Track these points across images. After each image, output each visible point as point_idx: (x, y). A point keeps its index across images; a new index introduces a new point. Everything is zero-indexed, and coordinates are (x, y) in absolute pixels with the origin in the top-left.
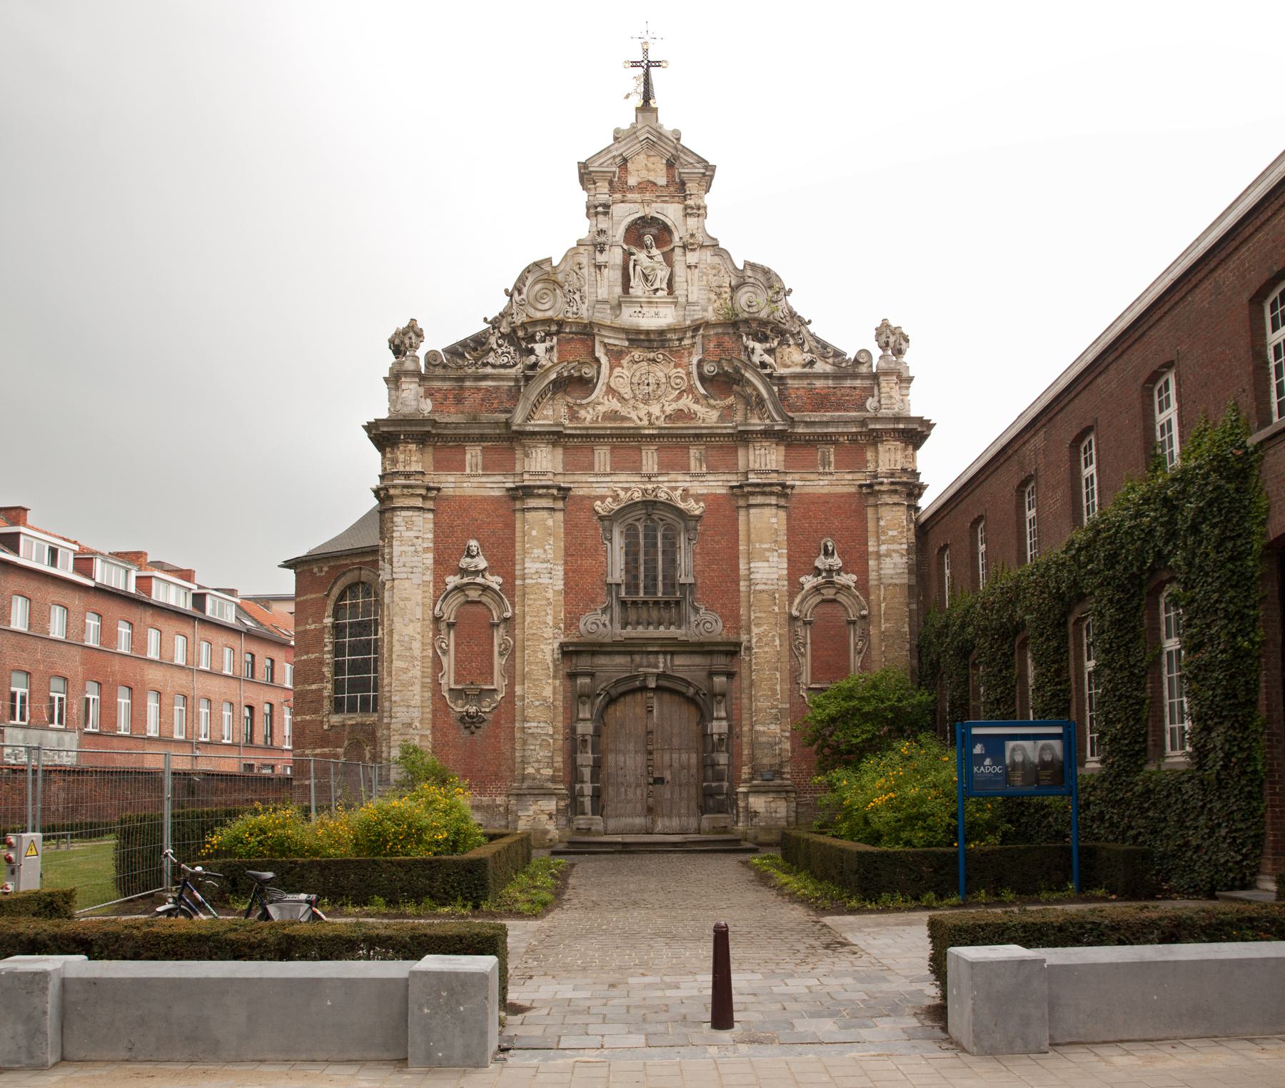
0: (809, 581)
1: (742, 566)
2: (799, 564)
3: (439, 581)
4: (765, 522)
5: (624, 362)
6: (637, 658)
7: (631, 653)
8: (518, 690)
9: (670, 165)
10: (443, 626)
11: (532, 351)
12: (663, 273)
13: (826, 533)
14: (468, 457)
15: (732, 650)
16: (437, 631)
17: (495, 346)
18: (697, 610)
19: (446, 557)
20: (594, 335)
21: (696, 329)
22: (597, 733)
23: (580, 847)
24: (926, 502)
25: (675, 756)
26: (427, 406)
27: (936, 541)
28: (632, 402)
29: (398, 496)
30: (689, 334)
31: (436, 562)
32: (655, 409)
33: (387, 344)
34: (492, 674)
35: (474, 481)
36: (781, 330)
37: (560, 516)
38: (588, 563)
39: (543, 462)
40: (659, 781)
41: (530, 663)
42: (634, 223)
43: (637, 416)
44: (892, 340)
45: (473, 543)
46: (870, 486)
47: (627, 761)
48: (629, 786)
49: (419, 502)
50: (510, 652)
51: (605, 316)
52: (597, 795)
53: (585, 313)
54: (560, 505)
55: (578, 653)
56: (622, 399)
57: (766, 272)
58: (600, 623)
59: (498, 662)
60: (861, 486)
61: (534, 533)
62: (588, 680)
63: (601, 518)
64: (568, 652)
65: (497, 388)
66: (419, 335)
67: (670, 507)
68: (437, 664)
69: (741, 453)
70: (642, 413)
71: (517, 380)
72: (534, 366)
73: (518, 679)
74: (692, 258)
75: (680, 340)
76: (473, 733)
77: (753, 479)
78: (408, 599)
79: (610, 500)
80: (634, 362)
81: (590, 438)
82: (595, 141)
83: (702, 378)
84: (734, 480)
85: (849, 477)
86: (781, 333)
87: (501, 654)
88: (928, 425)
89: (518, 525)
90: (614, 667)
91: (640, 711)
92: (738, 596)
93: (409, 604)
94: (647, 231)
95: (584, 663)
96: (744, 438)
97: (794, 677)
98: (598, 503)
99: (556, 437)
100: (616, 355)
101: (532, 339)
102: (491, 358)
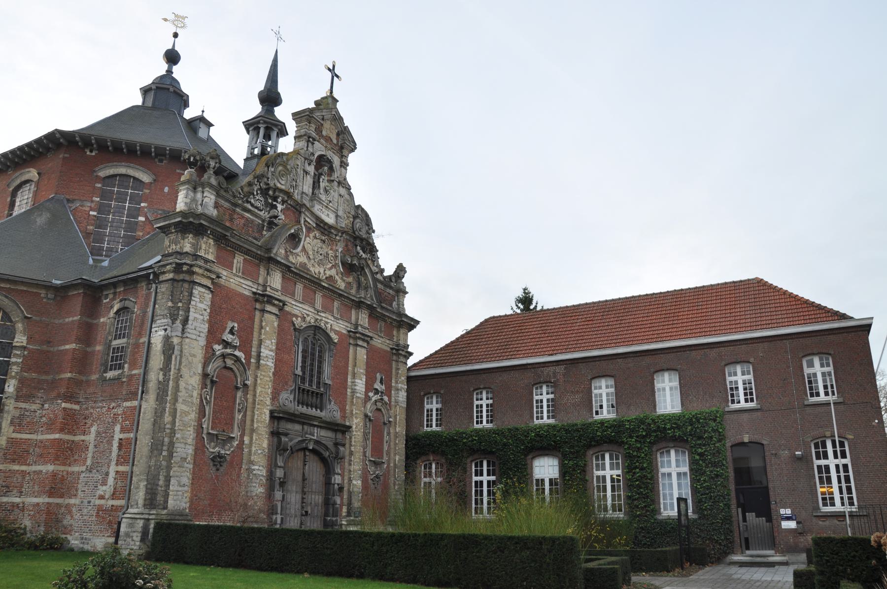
1: (349, 380)
3: (209, 348)
5: (311, 235)
6: (306, 427)
7: (303, 424)
10: (208, 382)
11: (275, 207)
14: (235, 261)
15: (344, 429)
16: (204, 386)
18: (330, 401)
20: (300, 212)
29: (198, 274)
31: (209, 331)
34: (232, 425)
38: (286, 357)
41: (258, 422)
43: (316, 270)
49: (208, 283)
55: (279, 419)
57: (367, 215)
59: (238, 417)
60: (392, 349)
61: (268, 329)
63: (295, 329)
65: (253, 221)
70: (317, 271)
71: (263, 221)
73: (247, 432)
76: (218, 470)
78: (194, 356)
79: (299, 319)
80: (315, 237)
87: (239, 411)
91: (300, 464)
93: (195, 360)
96: (359, 305)
98: (294, 319)
100: (309, 230)
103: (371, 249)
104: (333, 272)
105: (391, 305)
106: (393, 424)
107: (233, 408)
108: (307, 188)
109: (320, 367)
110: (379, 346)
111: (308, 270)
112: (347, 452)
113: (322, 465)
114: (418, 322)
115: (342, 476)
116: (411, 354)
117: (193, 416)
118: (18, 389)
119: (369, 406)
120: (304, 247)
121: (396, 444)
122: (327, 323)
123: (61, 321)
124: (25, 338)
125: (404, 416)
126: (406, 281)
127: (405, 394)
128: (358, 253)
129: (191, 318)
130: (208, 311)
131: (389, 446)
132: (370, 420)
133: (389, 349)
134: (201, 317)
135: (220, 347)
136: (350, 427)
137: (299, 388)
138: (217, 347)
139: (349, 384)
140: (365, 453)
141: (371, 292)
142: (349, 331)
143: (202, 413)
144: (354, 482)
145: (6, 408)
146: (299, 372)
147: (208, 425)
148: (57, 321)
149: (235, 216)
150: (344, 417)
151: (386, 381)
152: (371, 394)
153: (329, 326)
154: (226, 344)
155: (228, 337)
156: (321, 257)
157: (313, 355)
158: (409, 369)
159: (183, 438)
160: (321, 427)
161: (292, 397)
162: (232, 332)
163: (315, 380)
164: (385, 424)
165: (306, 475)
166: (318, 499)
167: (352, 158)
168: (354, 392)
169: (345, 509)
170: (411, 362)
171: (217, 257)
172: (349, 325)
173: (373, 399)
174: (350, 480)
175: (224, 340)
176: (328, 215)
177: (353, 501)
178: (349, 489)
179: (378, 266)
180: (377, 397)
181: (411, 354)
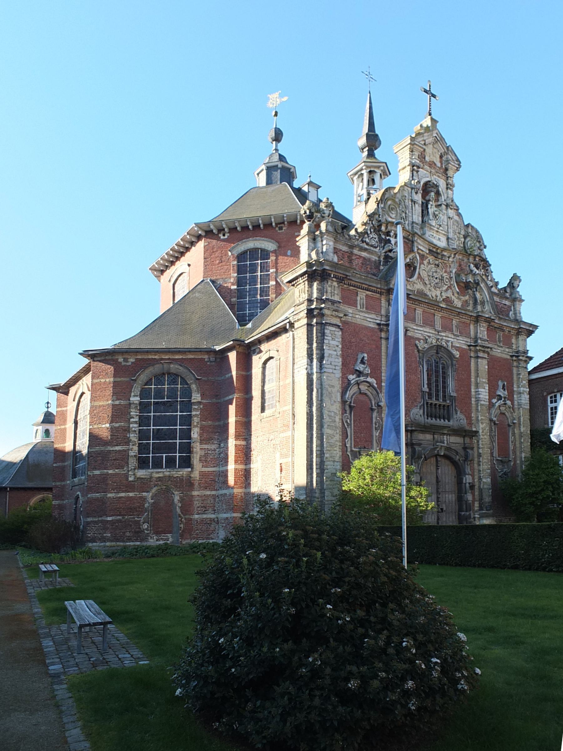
1: (473, 390)
3: (344, 377)
5: (425, 262)
10: (347, 408)
14: (359, 298)
16: (344, 411)
17: (369, 232)
20: (413, 242)
25: (447, 495)
28: (429, 286)
30: (453, 256)
46: (517, 357)
48: (429, 514)
49: (337, 321)
57: (477, 232)
59: (376, 434)
60: (512, 356)
63: (419, 351)
75: (449, 257)
78: (333, 386)
85: (507, 350)
87: (376, 429)
91: (433, 468)
92: (471, 407)
98: (417, 342)
103: (484, 264)
104: (449, 294)
105: (508, 315)
106: (517, 425)
107: (372, 427)
108: (417, 218)
109: (444, 382)
110: (499, 355)
111: (426, 295)
112: (476, 455)
113: (453, 468)
114: (536, 327)
115: (473, 476)
116: (531, 358)
117: (338, 437)
118: (201, 435)
119: (493, 411)
120: (419, 274)
121: (521, 443)
122: (448, 341)
123: (223, 378)
124: (199, 395)
125: (528, 417)
126: (522, 290)
127: (528, 397)
128: (472, 271)
129: (325, 355)
130: (340, 346)
131: (515, 445)
132: (495, 424)
133: (509, 357)
134: (335, 353)
135: (354, 376)
136: (477, 432)
137: (427, 403)
138: (351, 377)
139: (473, 393)
140: (492, 454)
141: (487, 307)
142: (469, 346)
143: (345, 435)
144: (484, 480)
145: (195, 450)
146: (426, 389)
147: (351, 444)
148: (219, 379)
149: (354, 258)
150: (470, 424)
151: (509, 388)
152: (494, 401)
153: (450, 344)
154: (359, 373)
155: (360, 367)
156: (437, 281)
157: (437, 372)
158: (530, 373)
159: (331, 457)
160: (450, 435)
161: (422, 411)
162: (362, 362)
163: (441, 394)
164: (509, 426)
165: (440, 479)
166: (451, 497)
167: (457, 178)
168: (478, 400)
169: (477, 504)
170: (531, 366)
171: (342, 298)
172: (469, 340)
173: (497, 404)
174: (480, 479)
175: (357, 370)
176: (439, 239)
177: (484, 496)
178: (479, 487)
179: (492, 280)
180: (501, 402)
181: (531, 358)
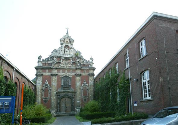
0: (83, 85)
2: (82, 83)
3: (43, 85)
4: (78, 78)
8: (51, 97)
9: (69, 40)
12: (68, 51)
13: (85, 79)
15: (75, 93)
16: (42, 91)
19: (43, 82)
21: (72, 57)
22: (60, 102)
23: (58, 116)
24: (95, 76)
26: (42, 65)
27: (96, 80)
32: (67, 66)
33: (38, 58)
35: (47, 74)
36: (80, 58)
37: (56, 78)
38: (59, 83)
39: (55, 72)
40: (67, 108)
42: (65, 46)
44: (92, 59)
45: (47, 81)
47: (63, 105)
50: (50, 93)
51: (62, 56)
52: (60, 110)
53: (60, 55)
54: (56, 76)
56: (63, 65)
57: (79, 52)
58: (60, 90)
62: (59, 96)
64: (57, 93)
66: (41, 57)
67: (68, 77)
68: (42, 95)
69: (76, 71)
72: (54, 61)
74: (71, 50)
77: (77, 74)
81: (60, 69)
82: (61, 36)
83: (72, 63)
84: (75, 74)
86: (80, 58)
88: (95, 68)
89: (52, 79)
90: (62, 95)
94: (67, 47)
95: (59, 94)
96: (76, 69)
97: (81, 95)
99: (56, 69)
101: (54, 58)
102: (49, 60)
